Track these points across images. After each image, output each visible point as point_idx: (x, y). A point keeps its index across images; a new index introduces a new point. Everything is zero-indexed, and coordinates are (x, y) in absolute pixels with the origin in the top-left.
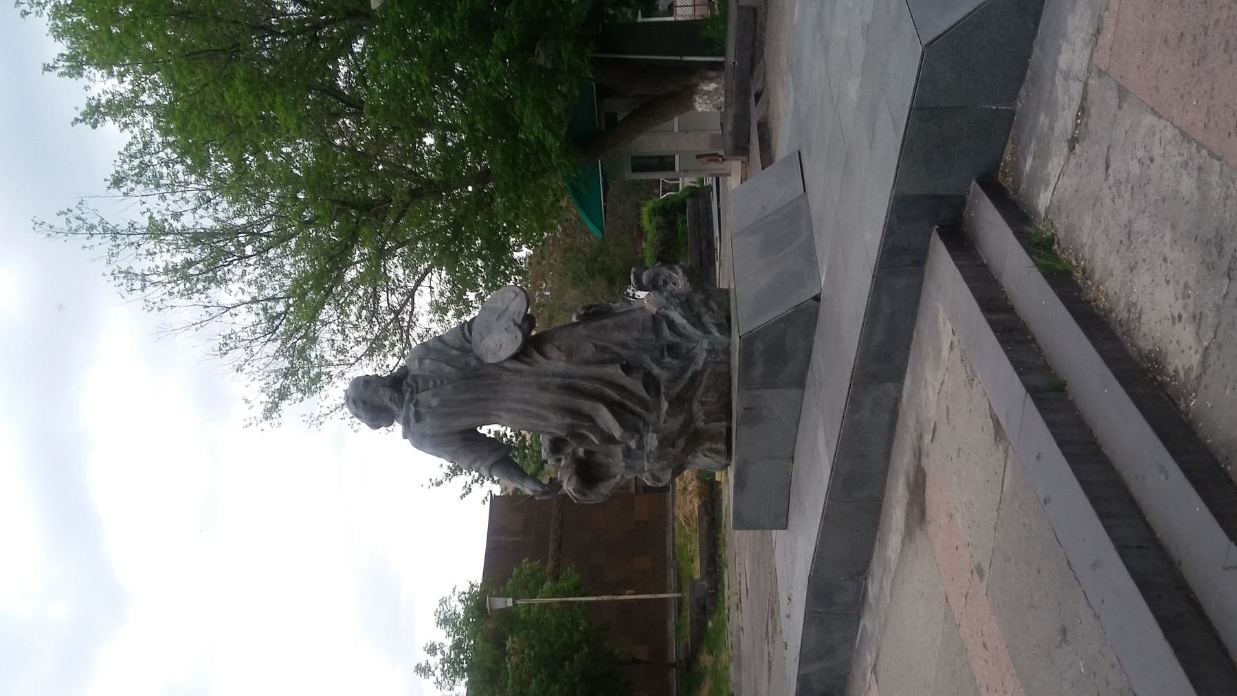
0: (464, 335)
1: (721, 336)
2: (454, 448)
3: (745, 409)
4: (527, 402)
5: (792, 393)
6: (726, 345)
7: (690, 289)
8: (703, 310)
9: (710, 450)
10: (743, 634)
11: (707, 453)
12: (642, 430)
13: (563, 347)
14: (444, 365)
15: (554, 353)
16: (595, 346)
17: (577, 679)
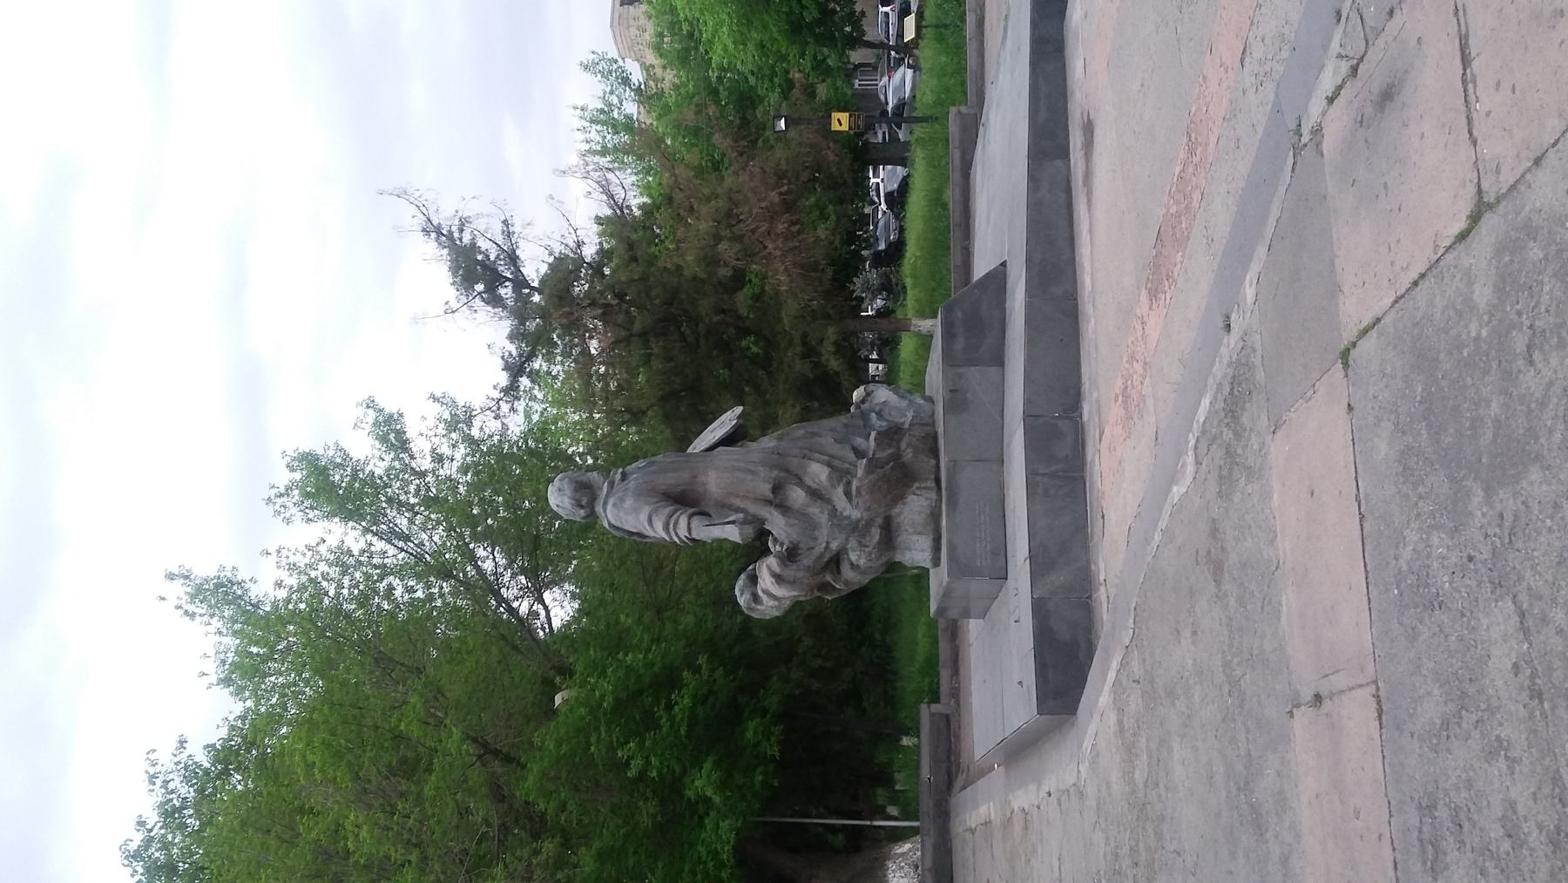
1: (925, 403)
2: (655, 500)
3: (951, 391)
4: (738, 460)
5: (993, 370)
6: (930, 413)
9: (918, 488)
11: (918, 492)
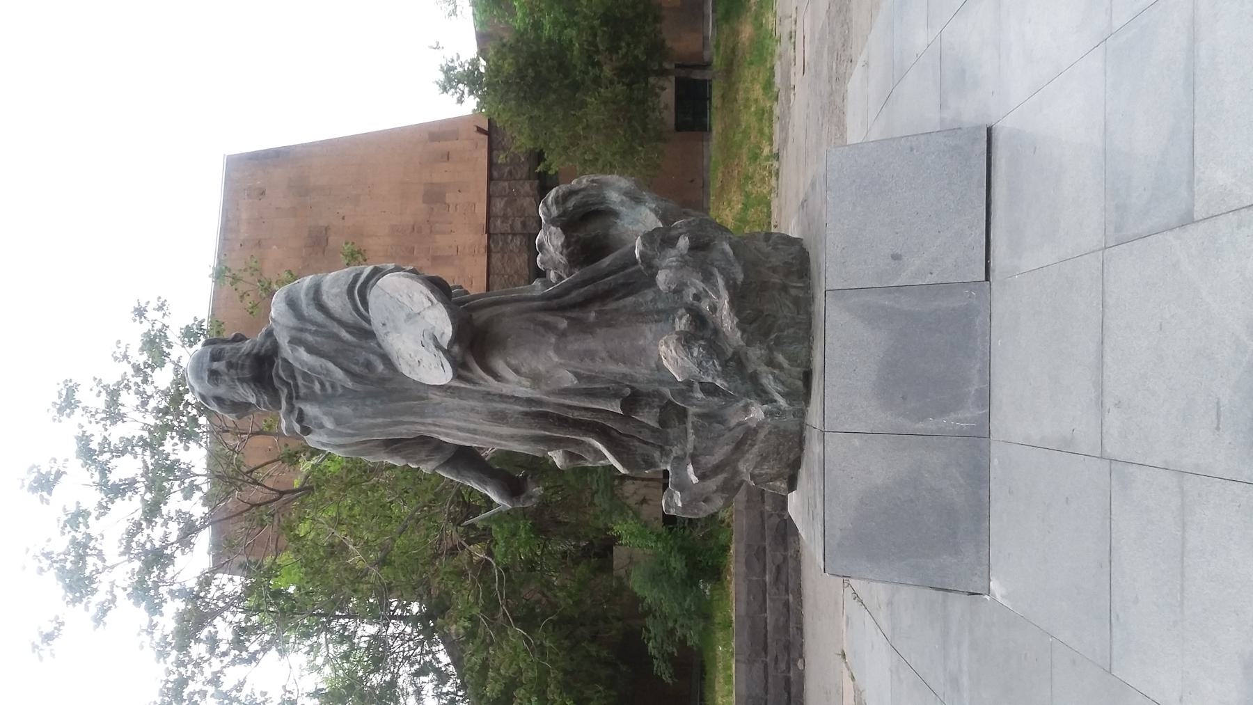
0: (356, 309)
7: (742, 343)
8: (763, 368)
10: (794, 94)
12: (657, 460)
13: (523, 370)
14: (331, 366)
15: (509, 374)
16: (577, 375)
17: (597, 23)
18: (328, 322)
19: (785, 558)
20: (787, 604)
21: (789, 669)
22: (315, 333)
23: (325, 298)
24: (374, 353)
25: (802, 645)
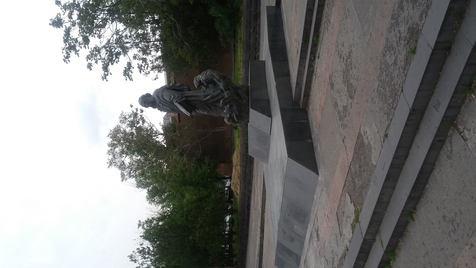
18: (166, 101)
19: (256, 25)
20: (256, 38)
21: (256, 54)
22: (163, 102)
23: (165, 98)
24: (175, 107)
25: (259, 48)
